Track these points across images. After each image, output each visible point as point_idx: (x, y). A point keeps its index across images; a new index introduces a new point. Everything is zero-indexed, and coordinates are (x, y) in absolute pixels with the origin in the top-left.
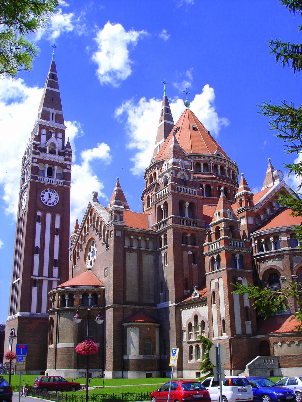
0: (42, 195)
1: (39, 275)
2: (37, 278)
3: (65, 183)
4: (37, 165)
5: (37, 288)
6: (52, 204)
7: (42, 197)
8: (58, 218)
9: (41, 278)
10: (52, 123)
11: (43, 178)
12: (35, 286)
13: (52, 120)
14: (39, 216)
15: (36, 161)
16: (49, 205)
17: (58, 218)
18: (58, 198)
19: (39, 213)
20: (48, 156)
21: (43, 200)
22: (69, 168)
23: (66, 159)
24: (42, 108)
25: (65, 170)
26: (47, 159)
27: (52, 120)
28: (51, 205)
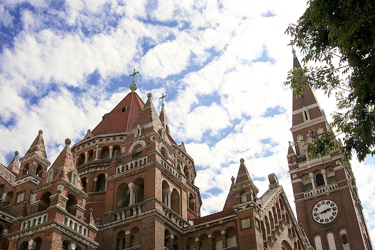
0: (315, 213)
3: (339, 185)
4: (299, 180)
6: (331, 219)
10: (308, 122)
11: (310, 193)
13: (307, 119)
15: (296, 176)
16: (327, 222)
18: (336, 208)
20: (309, 163)
21: (318, 219)
23: (332, 155)
25: (336, 169)
26: (308, 167)
27: (307, 119)
28: (330, 221)
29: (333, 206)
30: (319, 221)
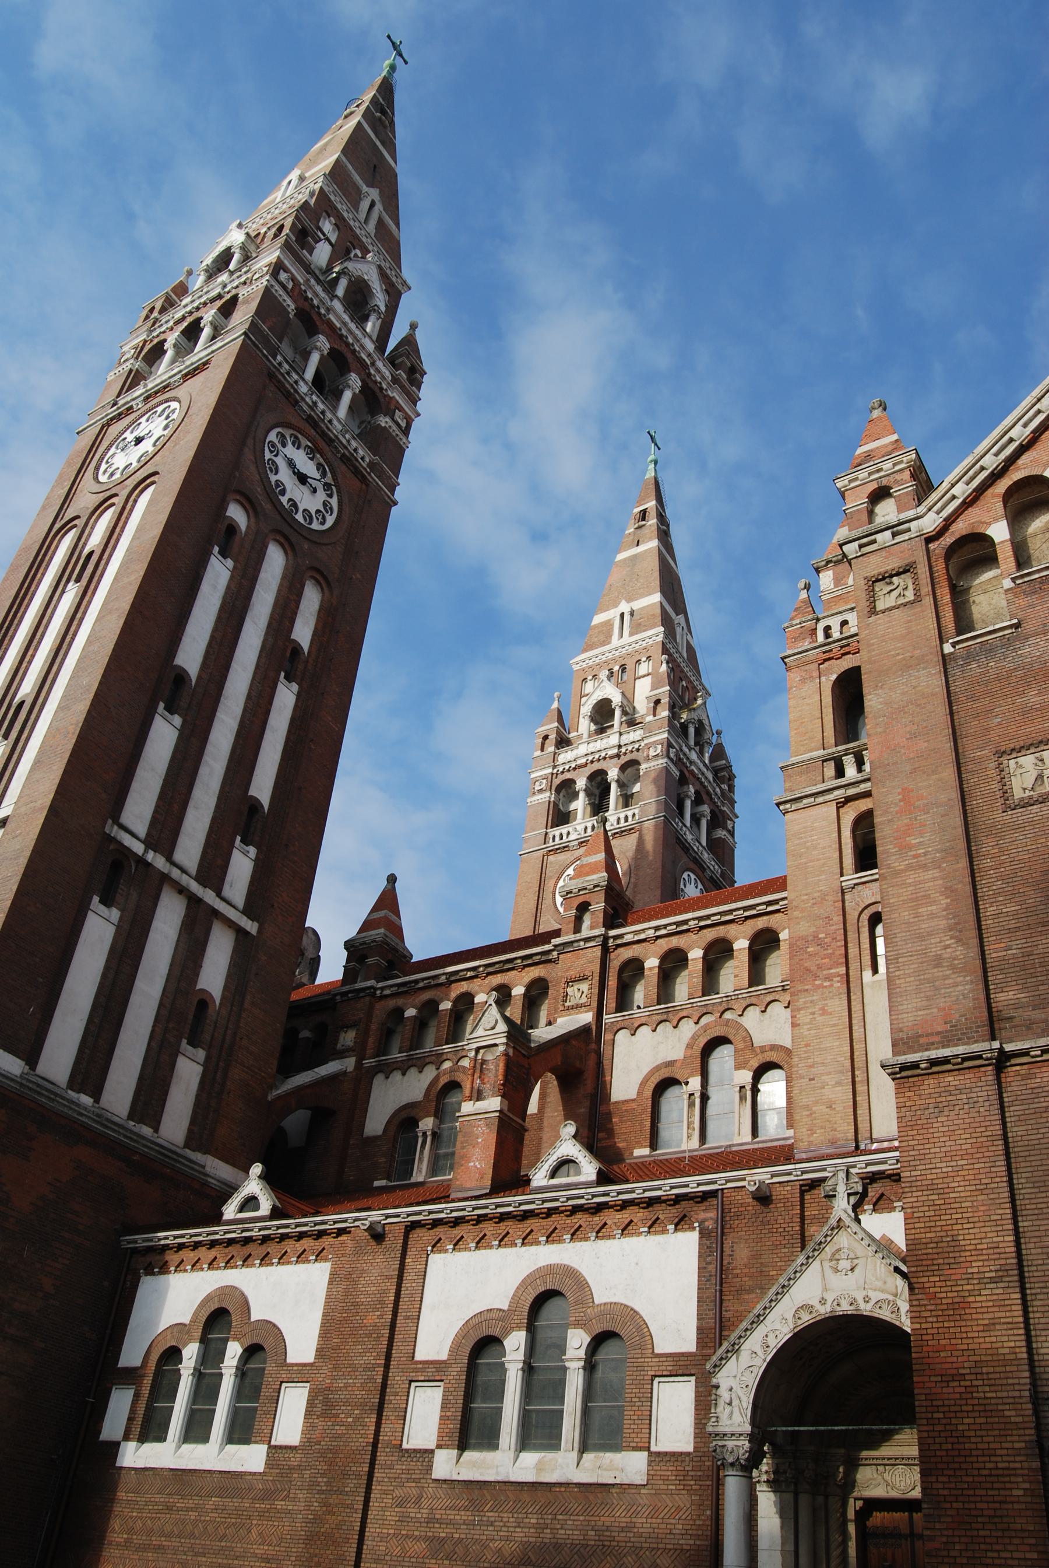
0: (273, 445)
1: (148, 834)
2: (138, 848)
5: (115, 914)
7: (272, 452)
8: (311, 599)
9: (158, 861)
12: (107, 901)
14: (232, 528)
17: (311, 599)
18: (331, 509)
19: (236, 513)
22: (403, 424)
24: (335, 157)
25: (384, 421)
28: (299, 517)
29: (330, 496)
30: (273, 478)
